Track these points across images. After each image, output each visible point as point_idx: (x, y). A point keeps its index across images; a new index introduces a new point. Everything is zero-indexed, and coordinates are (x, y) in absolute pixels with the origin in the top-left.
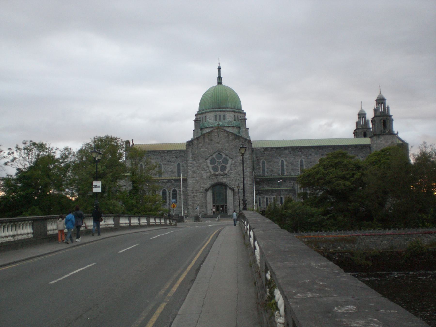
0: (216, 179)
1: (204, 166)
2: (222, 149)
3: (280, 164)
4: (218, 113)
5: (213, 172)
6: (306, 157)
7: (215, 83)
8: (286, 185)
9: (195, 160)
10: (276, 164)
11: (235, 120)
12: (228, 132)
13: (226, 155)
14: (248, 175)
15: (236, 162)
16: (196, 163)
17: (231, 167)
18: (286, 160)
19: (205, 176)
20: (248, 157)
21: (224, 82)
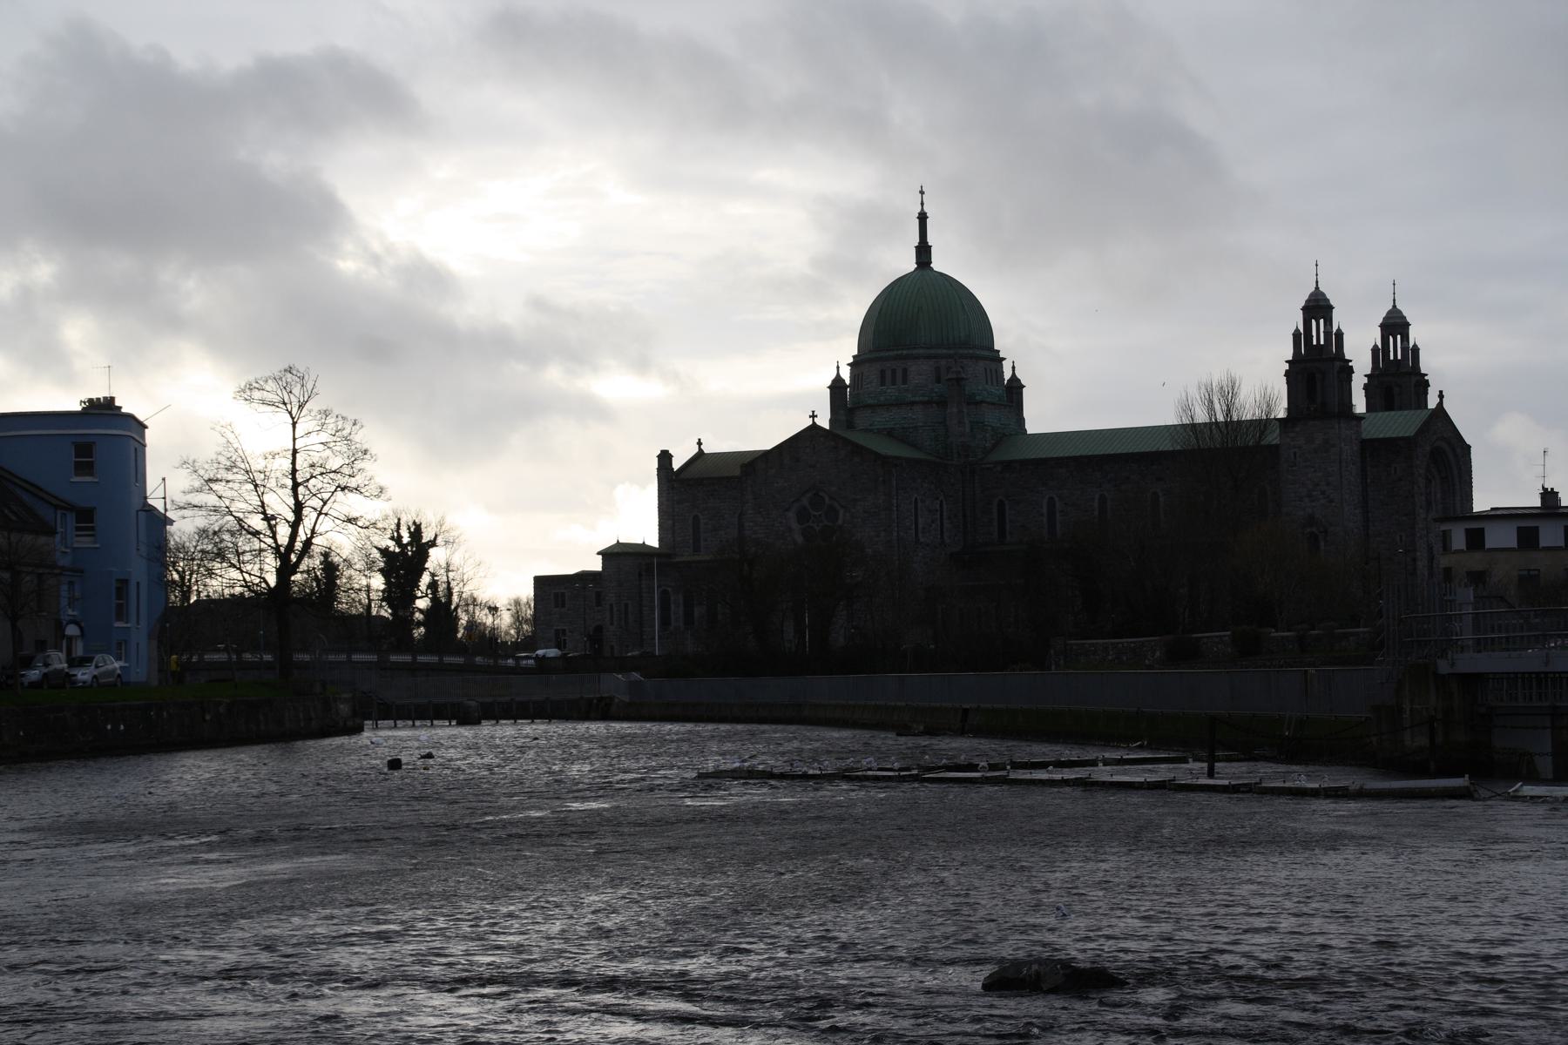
3: (1045, 510)
7: (909, 264)
21: (938, 264)
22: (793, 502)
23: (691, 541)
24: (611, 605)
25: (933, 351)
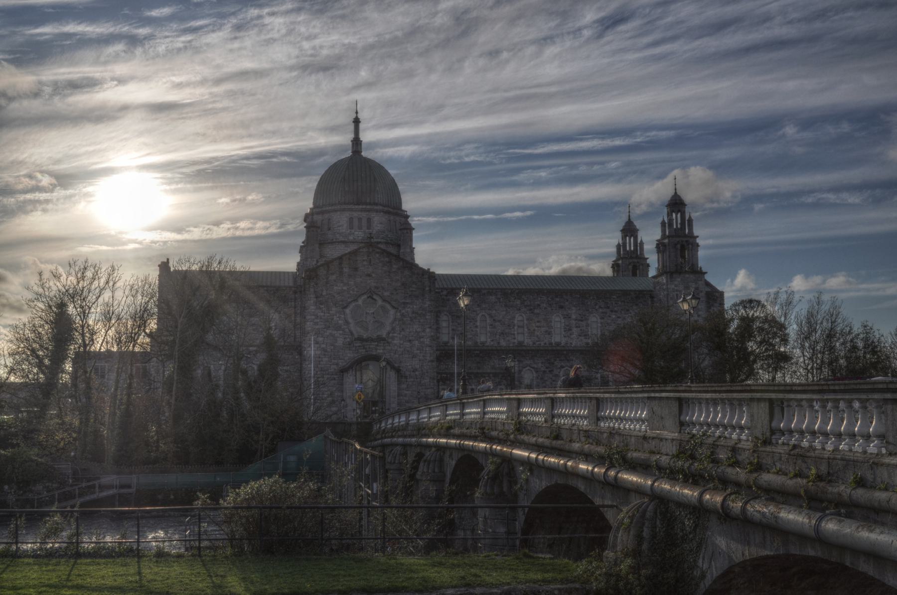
0: (364, 348)
1: (340, 322)
2: (377, 288)
4: (355, 214)
6: (531, 310)
8: (492, 364)
10: (470, 322)
13: (384, 300)
14: (428, 343)
15: (403, 315)
16: (322, 314)
17: (394, 325)
18: (491, 316)
19: (340, 342)
20: (427, 305)
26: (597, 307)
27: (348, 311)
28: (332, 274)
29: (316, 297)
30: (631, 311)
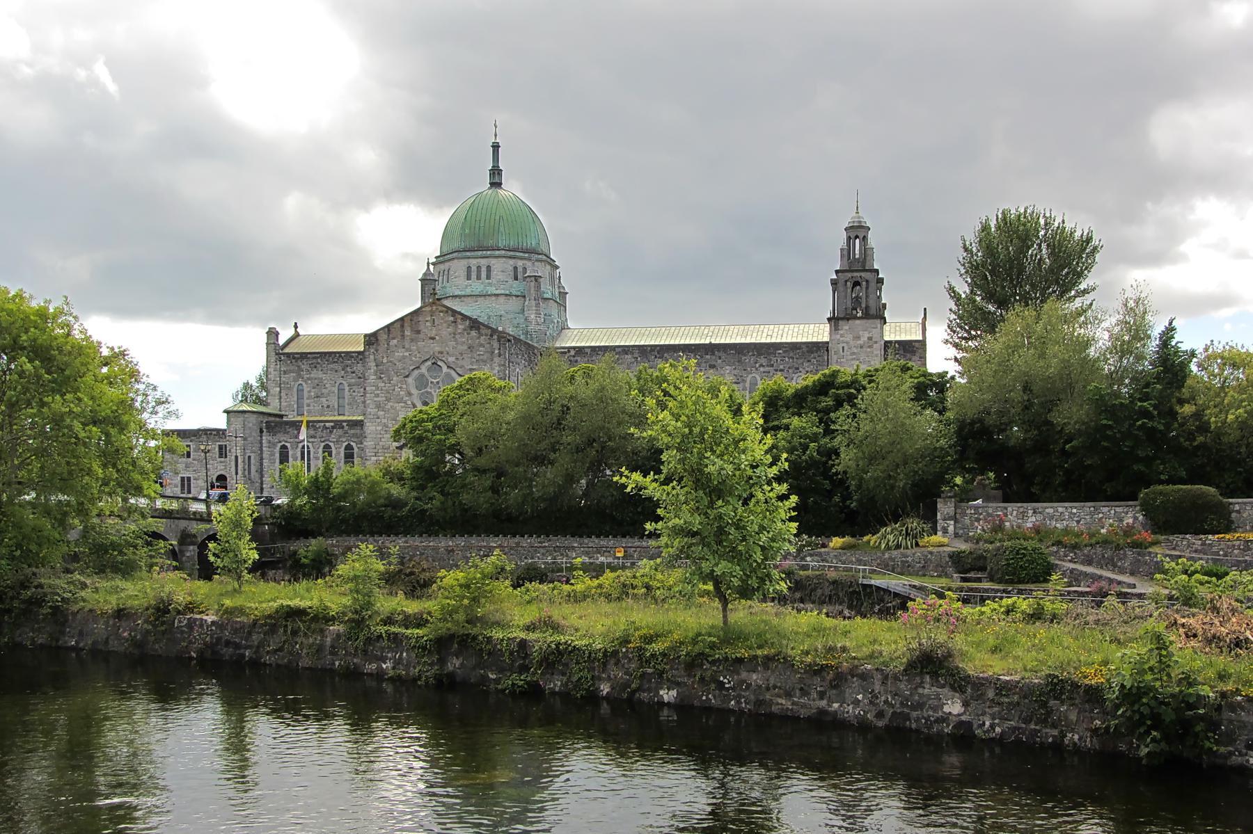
2: (442, 353)
4: (473, 262)
5: (419, 407)
9: (381, 378)
11: (516, 278)
12: (454, 312)
16: (383, 384)
22: (413, 370)
23: (295, 406)
24: (236, 457)
25: (512, 253)
26: (757, 365)
27: (410, 380)
28: (394, 338)
29: (377, 366)
30: (801, 369)
